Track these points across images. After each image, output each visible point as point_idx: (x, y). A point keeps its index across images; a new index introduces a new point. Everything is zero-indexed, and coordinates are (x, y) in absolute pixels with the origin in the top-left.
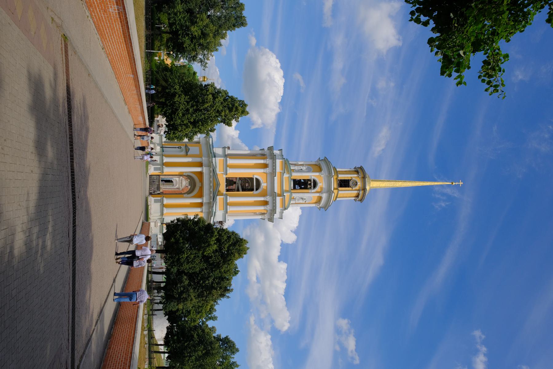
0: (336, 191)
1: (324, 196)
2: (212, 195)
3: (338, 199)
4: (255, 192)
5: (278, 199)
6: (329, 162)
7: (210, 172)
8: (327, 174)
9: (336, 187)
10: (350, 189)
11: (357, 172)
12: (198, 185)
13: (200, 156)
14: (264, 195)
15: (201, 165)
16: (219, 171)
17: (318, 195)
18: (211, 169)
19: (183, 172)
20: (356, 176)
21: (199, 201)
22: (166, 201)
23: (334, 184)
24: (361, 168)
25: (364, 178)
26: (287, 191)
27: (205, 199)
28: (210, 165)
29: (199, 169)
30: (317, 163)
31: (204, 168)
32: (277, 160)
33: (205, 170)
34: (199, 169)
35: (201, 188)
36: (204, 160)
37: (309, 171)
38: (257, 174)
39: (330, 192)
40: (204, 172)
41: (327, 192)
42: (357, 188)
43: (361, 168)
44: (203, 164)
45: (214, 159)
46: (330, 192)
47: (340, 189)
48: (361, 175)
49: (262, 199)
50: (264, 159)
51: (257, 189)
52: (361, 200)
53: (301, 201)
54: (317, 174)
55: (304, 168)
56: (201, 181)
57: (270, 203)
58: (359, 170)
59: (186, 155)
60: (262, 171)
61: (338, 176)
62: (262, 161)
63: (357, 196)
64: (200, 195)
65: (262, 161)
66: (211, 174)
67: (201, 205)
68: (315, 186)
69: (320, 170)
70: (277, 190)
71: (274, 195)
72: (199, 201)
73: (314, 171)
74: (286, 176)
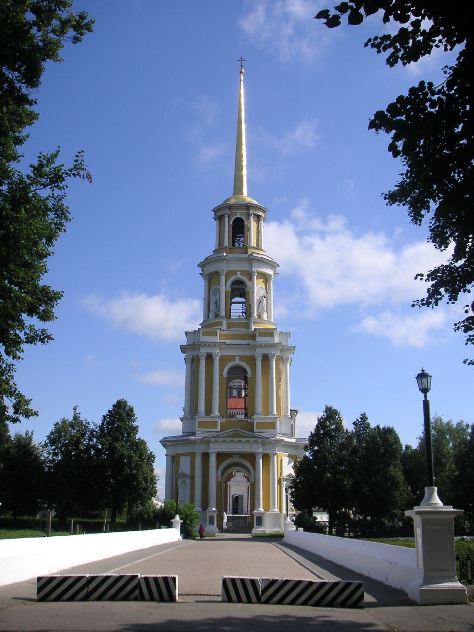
0: (250, 251)
2: (251, 440)
4: (249, 375)
6: (206, 259)
7: (216, 441)
8: (224, 264)
12: (236, 459)
13: (193, 456)
14: (252, 360)
15: (206, 456)
18: (213, 440)
20: (226, 219)
24: (216, 211)
25: (230, 207)
28: (206, 441)
29: (213, 459)
30: (207, 279)
31: (211, 450)
32: (201, 340)
33: (215, 448)
34: (213, 459)
35: (242, 455)
36: (199, 449)
40: (216, 450)
43: (216, 211)
49: (259, 363)
51: (246, 371)
54: (223, 278)
55: (213, 299)
58: (218, 214)
61: (226, 247)
62: (203, 363)
64: (251, 457)
65: (203, 363)
66: (220, 440)
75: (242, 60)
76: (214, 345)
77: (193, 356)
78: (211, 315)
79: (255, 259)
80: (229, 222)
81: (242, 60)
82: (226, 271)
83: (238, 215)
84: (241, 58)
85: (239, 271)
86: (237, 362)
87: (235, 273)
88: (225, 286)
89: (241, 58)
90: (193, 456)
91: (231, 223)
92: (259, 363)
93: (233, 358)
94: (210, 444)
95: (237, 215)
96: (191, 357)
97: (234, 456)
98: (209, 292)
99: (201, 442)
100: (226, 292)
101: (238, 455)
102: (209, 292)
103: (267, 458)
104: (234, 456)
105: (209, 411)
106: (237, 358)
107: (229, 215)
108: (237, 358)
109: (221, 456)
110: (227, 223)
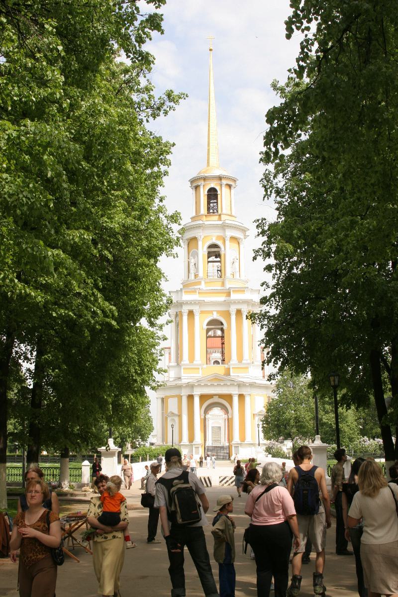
0: (223, 217)
1: (229, 233)
3: (233, 214)
4: (225, 327)
5: (234, 296)
7: (199, 385)
8: (201, 231)
9: (216, 218)
11: (197, 188)
12: (216, 399)
13: (180, 398)
14: (227, 314)
15: (191, 397)
16: (199, 375)
17: (227, 242)
19: (201, 419)
20: (202, 189)
21: (236, 399)
22: (236, 439)
23: (213, 220)
24: (192, 181)
25: (205, 179)
26: (223, 284)
27: (234, 391)
28: (191, 386)
29: (197, 400)
31: (194, 393)
33: (197, 392)
34: (197, 400)
35: (221, 396)
36: (185, 393)
37: (196, 255)
38: (201, 323)
39: (224, 227)
40: (199, 393)
41: (224, 230)
42: (218, 188)
43: (192, 181)
44: (190, 394)
45: (183, 381)
46: (224, 227)
47: (220, 212)
48: (201, 183)
49: (233, 317)
50: (182, 316)
51: (222, 324)
52: (235, 181)
53: (237, 264)
54: (200, 243)
55: (192, 261)
56: (211, 396)
57: (239, 307)
59: (180, 416)
60: (197, 318)
62: (185, 318)
63: (230, 186)
65: (185, 318)
67: (241, 397)
68: (215, 246)
69: (194, 239)
70: (222, 298)
71: (228, 303)
72: (236, 399)
73: (197, 248)
74: (203, 286)
76: (195, 303)
77: (177, 312)
78: (192, 277)
79: (227, 226)
82: (202, 237)
90: (180, 398)
91: (206, 193)
92: (233, 317)
94: (195, 389)
98: (189, 256)
99: (186, 386)
102: (189, 256)
103: (241, 397)
105: (192, 358)
109: (203, 398)
110: (204, 193)
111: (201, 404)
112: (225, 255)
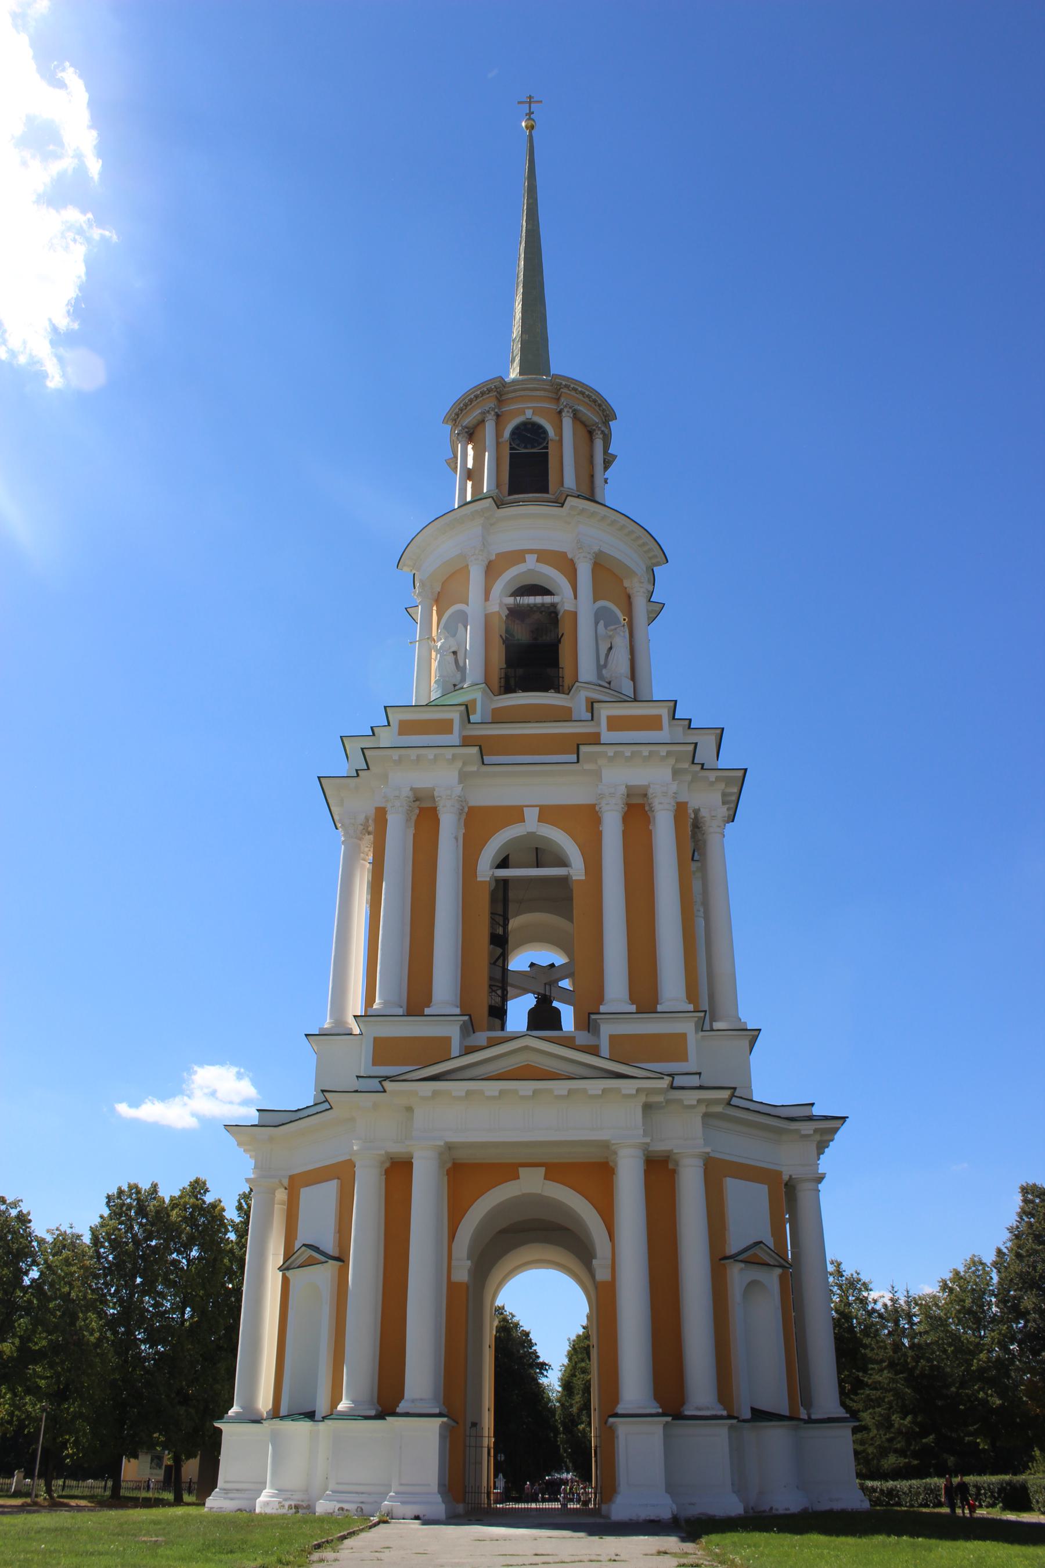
10: (552, 451)
15: (398, 1171)
20: (490, 427)
44: (397, 1149)
75: (530, 101)
80: (498, 434)
81: (530, 101)
83: (529, 414)
84: (530, 97)
85: (531, 551)
86: (531, 824)
87: (519, 556)
88: (487, 598)
89: (530, 97)
91: (507, 434)
93: (515, 814)
95: (524, 413)
96: (361, 818)
97: (522, 1171)
100: (487, 618)
101: (542, 1170)
104: (521, 1170)
106: (531, 815)
107: (498, 416)
108: (531, 815)
111: (455, 1212)
112: (575, 615)
